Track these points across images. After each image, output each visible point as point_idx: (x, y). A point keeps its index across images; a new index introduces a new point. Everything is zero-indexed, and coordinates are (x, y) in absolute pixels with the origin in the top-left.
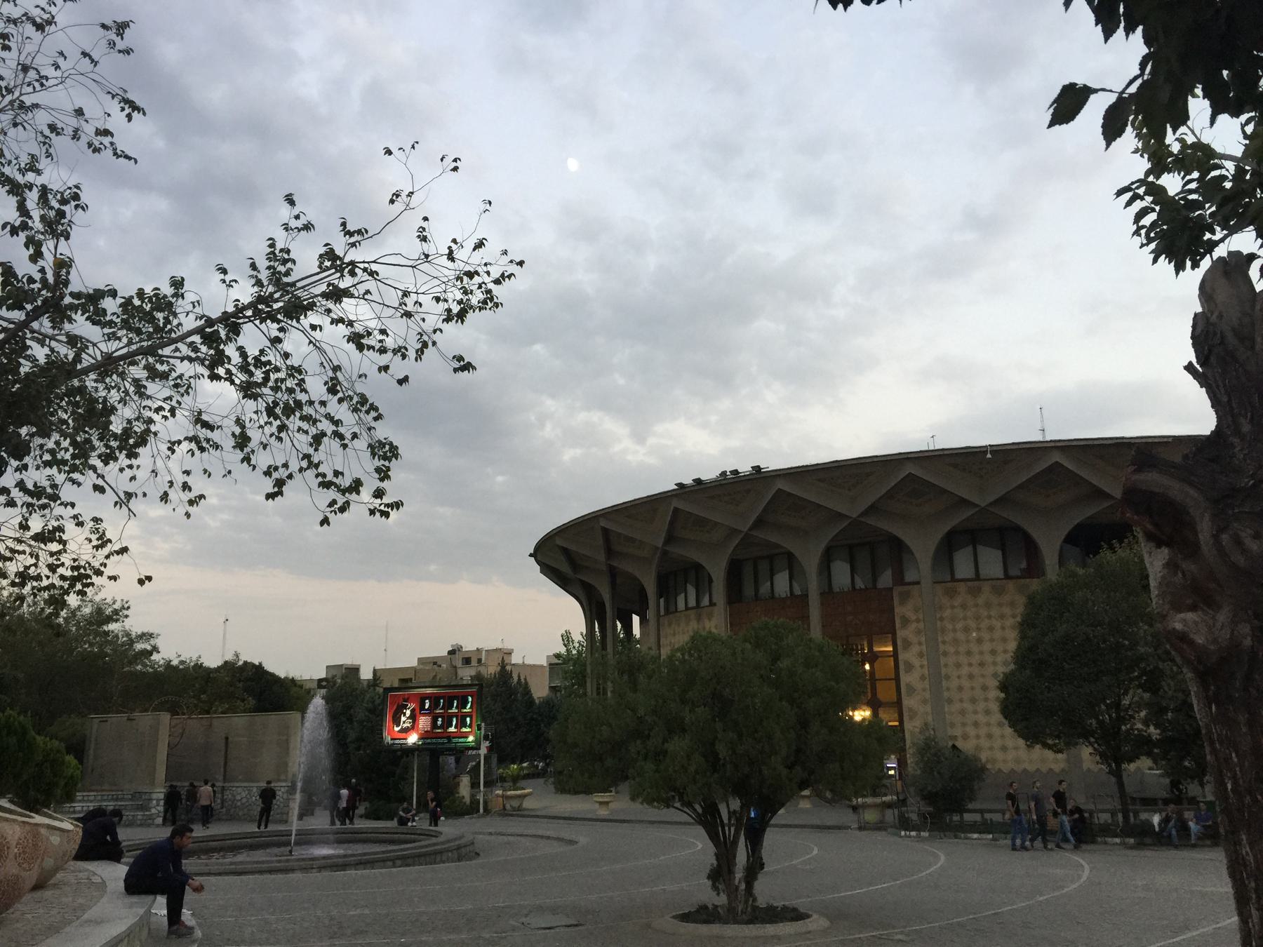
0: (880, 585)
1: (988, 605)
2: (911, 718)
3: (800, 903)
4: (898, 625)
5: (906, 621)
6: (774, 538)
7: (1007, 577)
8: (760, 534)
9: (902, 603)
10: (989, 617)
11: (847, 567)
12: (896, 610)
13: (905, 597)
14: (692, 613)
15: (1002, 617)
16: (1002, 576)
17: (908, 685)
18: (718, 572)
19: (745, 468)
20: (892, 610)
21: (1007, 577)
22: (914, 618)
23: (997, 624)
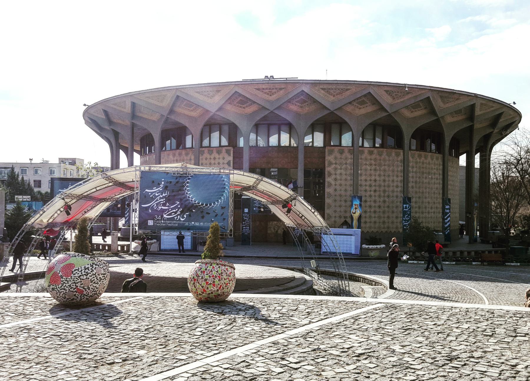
1: (366, 159)
5: (330, 164)
10: (366, 164)
13: (331, 152)
14: (206, 150)
15: (371, 165)
22: (334, 162)
23: (369, 168)
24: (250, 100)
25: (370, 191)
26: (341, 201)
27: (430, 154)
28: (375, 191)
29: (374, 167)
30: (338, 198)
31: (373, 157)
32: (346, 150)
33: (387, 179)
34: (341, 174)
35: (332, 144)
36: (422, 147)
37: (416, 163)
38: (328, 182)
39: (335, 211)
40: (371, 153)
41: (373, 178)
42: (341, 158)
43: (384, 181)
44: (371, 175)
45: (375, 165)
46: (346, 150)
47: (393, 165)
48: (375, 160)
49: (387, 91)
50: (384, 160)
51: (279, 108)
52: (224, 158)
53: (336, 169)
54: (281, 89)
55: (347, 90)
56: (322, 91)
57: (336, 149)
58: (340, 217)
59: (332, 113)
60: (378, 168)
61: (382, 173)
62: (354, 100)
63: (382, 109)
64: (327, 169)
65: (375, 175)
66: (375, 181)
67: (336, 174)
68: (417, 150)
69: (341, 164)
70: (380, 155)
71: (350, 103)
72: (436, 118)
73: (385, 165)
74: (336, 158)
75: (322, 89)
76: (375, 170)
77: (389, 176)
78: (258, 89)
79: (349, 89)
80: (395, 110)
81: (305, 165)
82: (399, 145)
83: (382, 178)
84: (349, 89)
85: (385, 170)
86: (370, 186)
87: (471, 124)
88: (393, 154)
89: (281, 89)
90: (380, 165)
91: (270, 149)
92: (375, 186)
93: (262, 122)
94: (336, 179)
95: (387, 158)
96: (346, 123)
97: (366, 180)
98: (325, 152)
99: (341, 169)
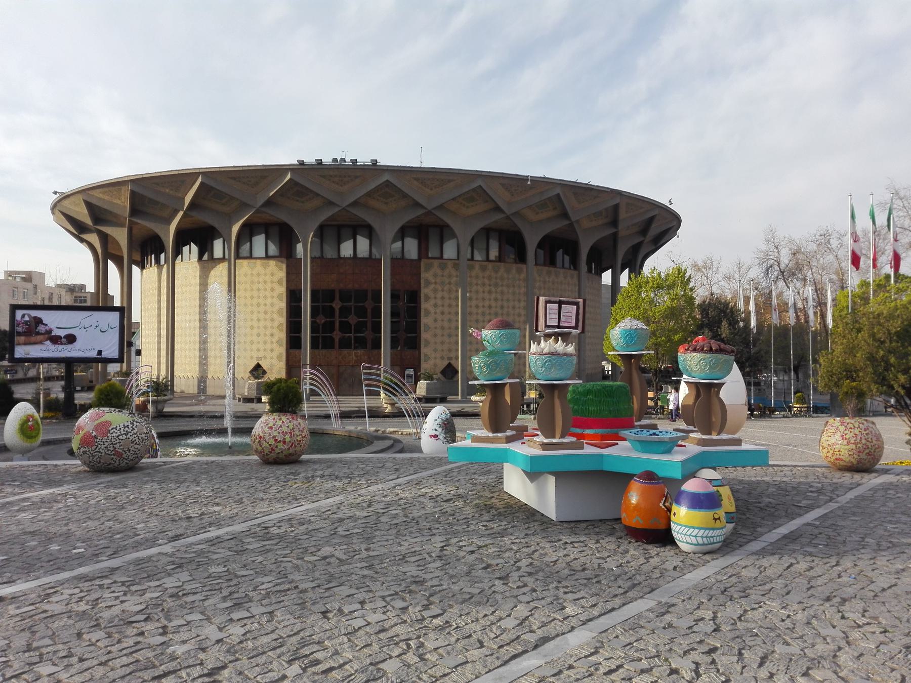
2: (426, 346)
3: (266, 470)
4: (422, 285)
5: (428, 283)
9: (427, 270)
10: (477, 284)
11: (367, 242)
12: (422, 275)
13: (429, 267)
16: (264, 255)
17: (425, 324)
19: (364, 159)
20: (420, 274)
24: (311, 191)
26: (443, 335)
27: (562, 271)
29: (487, 289)
30: (439, 332)
31: (487, 273)
32: (450, 264)
33: (505, 304)
34: (443, 298)
35: (430, 255)
36: (551, 262)
37: (545, 282)
38: (426, 310)
39: (435, 350)
40: (484, 269)
41: (487, 303)
42: (443, 276)
43: (502, 307)
44: (483, 299)
46: (450, 264)
47: (514, 286)
48: (490, 278)
49: (503, 185)
50: (502, 279)
52: (272, 275)
53: (435, 291)
54: (356, 177)
55: (450, 181)
56: (415, 182)
57: (436, 263)
58: (442, 358)
59: (429, 213)
60: (493, 289)
61: (499, 297)
62: (460, 196)
63: (498, 209)
64: (424, 291)
65: (490, 300)
66: (490, 307)
67: (435, 298)
68: (545, 265)
69: (443, 283)
71: (454, 199)
72: (567, 222)
73: (502, 286)
74: (435, 276)
75: (415, 179)
76: (490, 292)
77: (508, 300)
78: (324, 177)
79: (452, 180)
80: (514, 210)
81: (393, 285)
82: (521, 257)
83: (500, 303)
84: (452, 180)
85: (502, 293)
87: (614, 230)
88: (514, 271)
89: (356, 177)
90: (496, 285)
91: (342, 261)
92: (490, 314)
93: (329, 223)
94: (435, 305)
95: (505, 275)
96: (448, 226)
97: (477, 307)
98: (420, 267)
99: (443, 291)
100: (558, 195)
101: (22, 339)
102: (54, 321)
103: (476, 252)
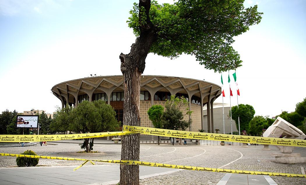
0: (122, 100)
6: (102, 90)
7: (145, 100)
8: (99, 89)
15: (143, 107)
18: (90, 96)
21: (145, 100)
25: (143, 118)
28: (145, 118)
29: (144, 108)
31: (144, 104)
44: (143, 111)
45: (145, 107)
48: (145, 105)
51: (99, 86)
54: (97, 80)
60: (146, 109)
70: (147, 103)
76: (145, 109)
78: (90, 81)
86: (143, 116)
89: (97, 80)
92: (145, 116)
100: (179, 81)
101: (19, 123)
102: (25, 119)
103: (118, 99)
